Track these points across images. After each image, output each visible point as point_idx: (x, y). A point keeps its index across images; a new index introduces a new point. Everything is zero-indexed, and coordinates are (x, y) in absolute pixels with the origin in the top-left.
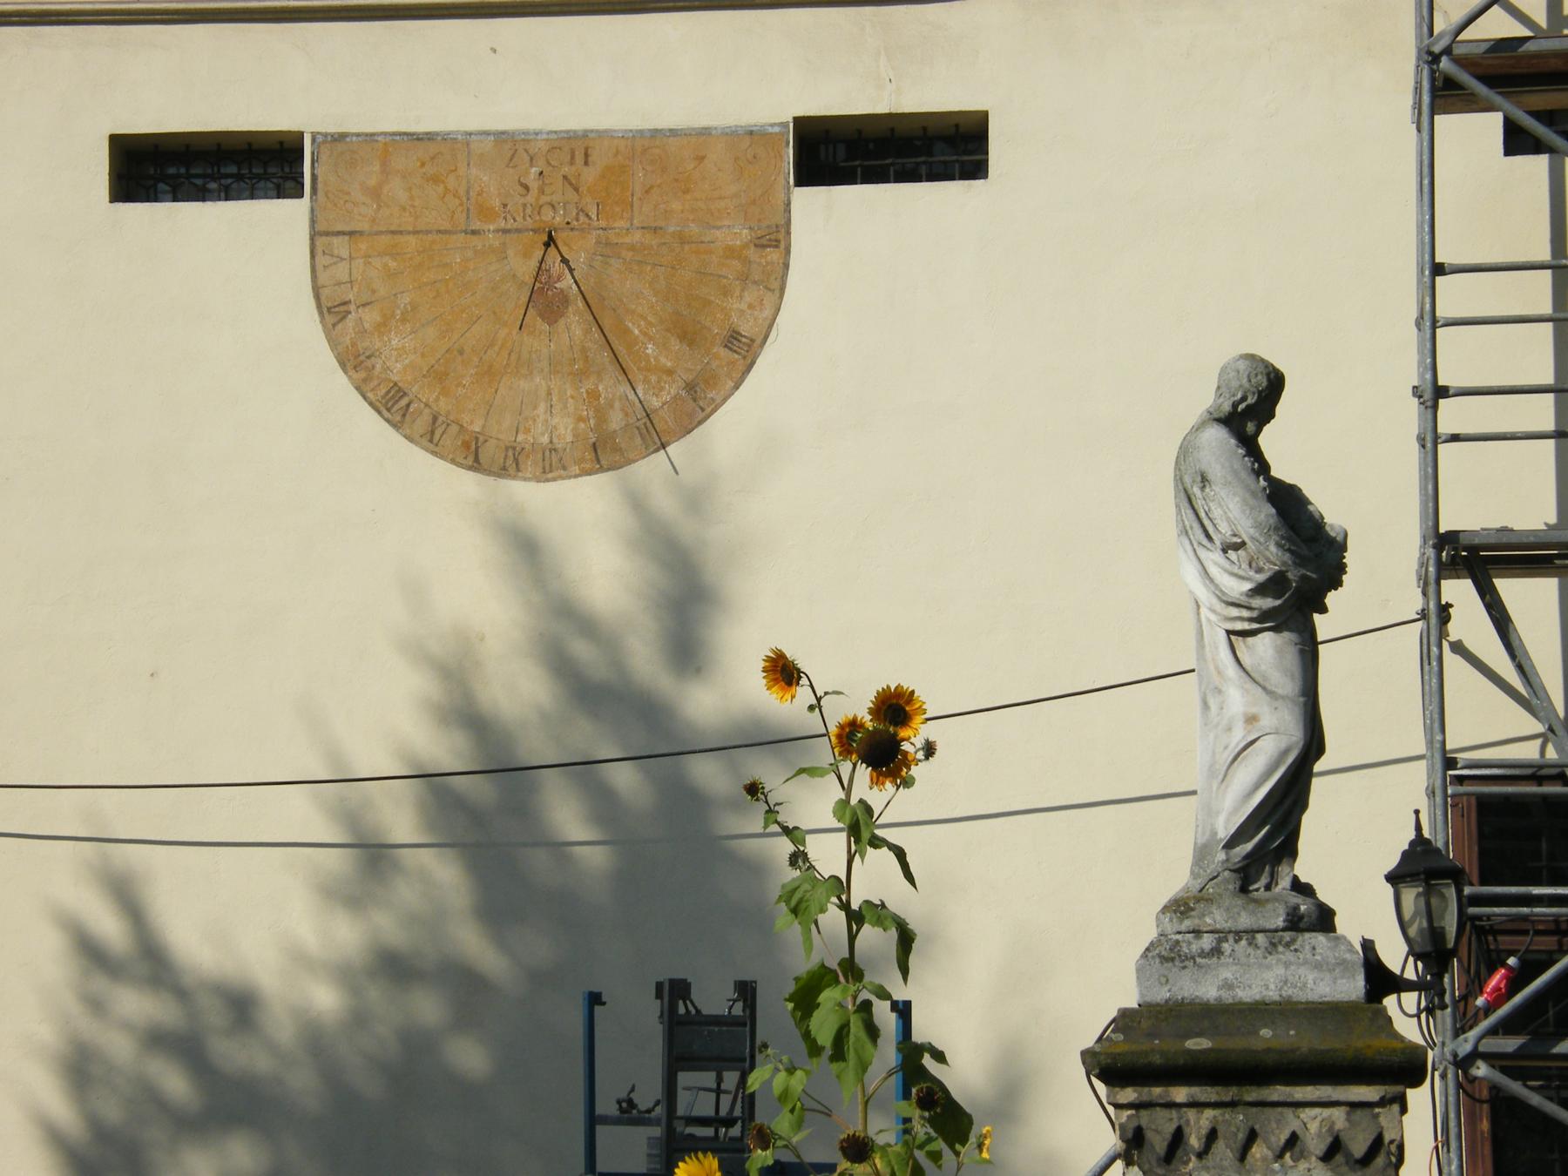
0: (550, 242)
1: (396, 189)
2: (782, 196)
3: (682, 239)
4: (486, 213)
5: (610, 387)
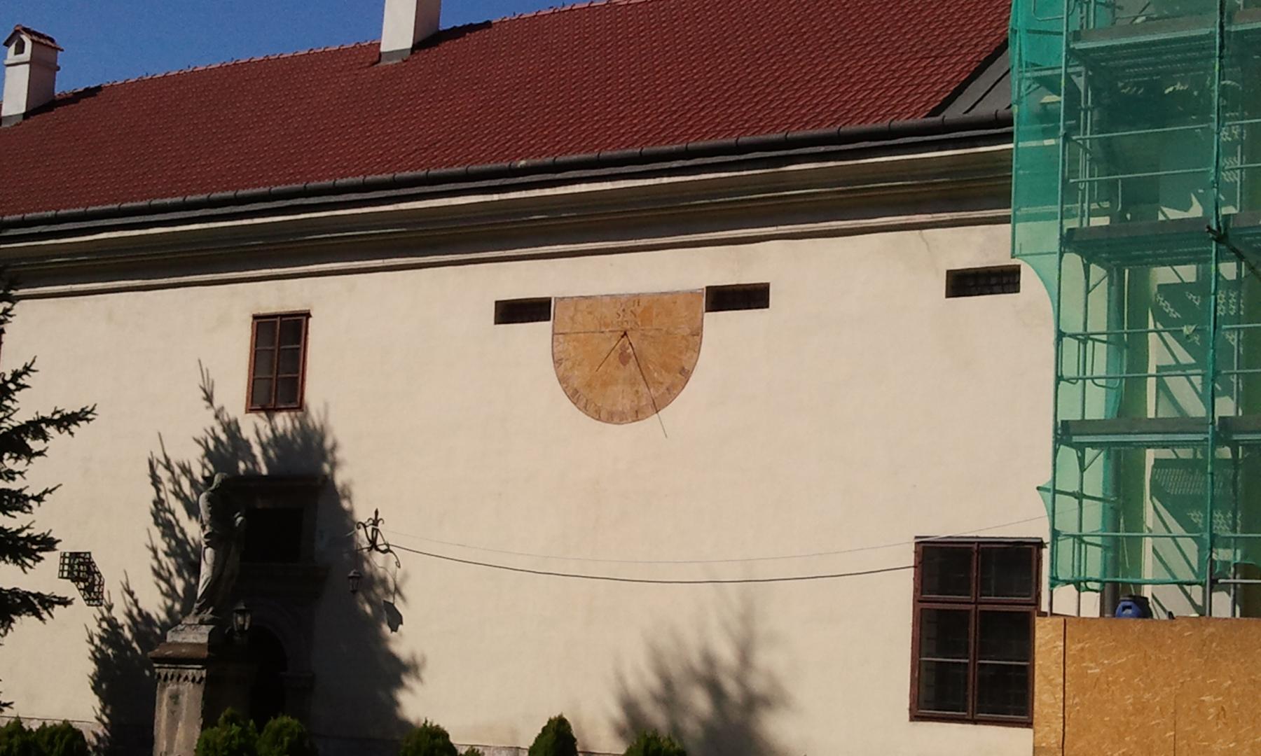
0: (625, 334)
1: (579, 317)
2: (700, 316)
3: (667, 332)
4: (606, 325)
5: (642, 388)
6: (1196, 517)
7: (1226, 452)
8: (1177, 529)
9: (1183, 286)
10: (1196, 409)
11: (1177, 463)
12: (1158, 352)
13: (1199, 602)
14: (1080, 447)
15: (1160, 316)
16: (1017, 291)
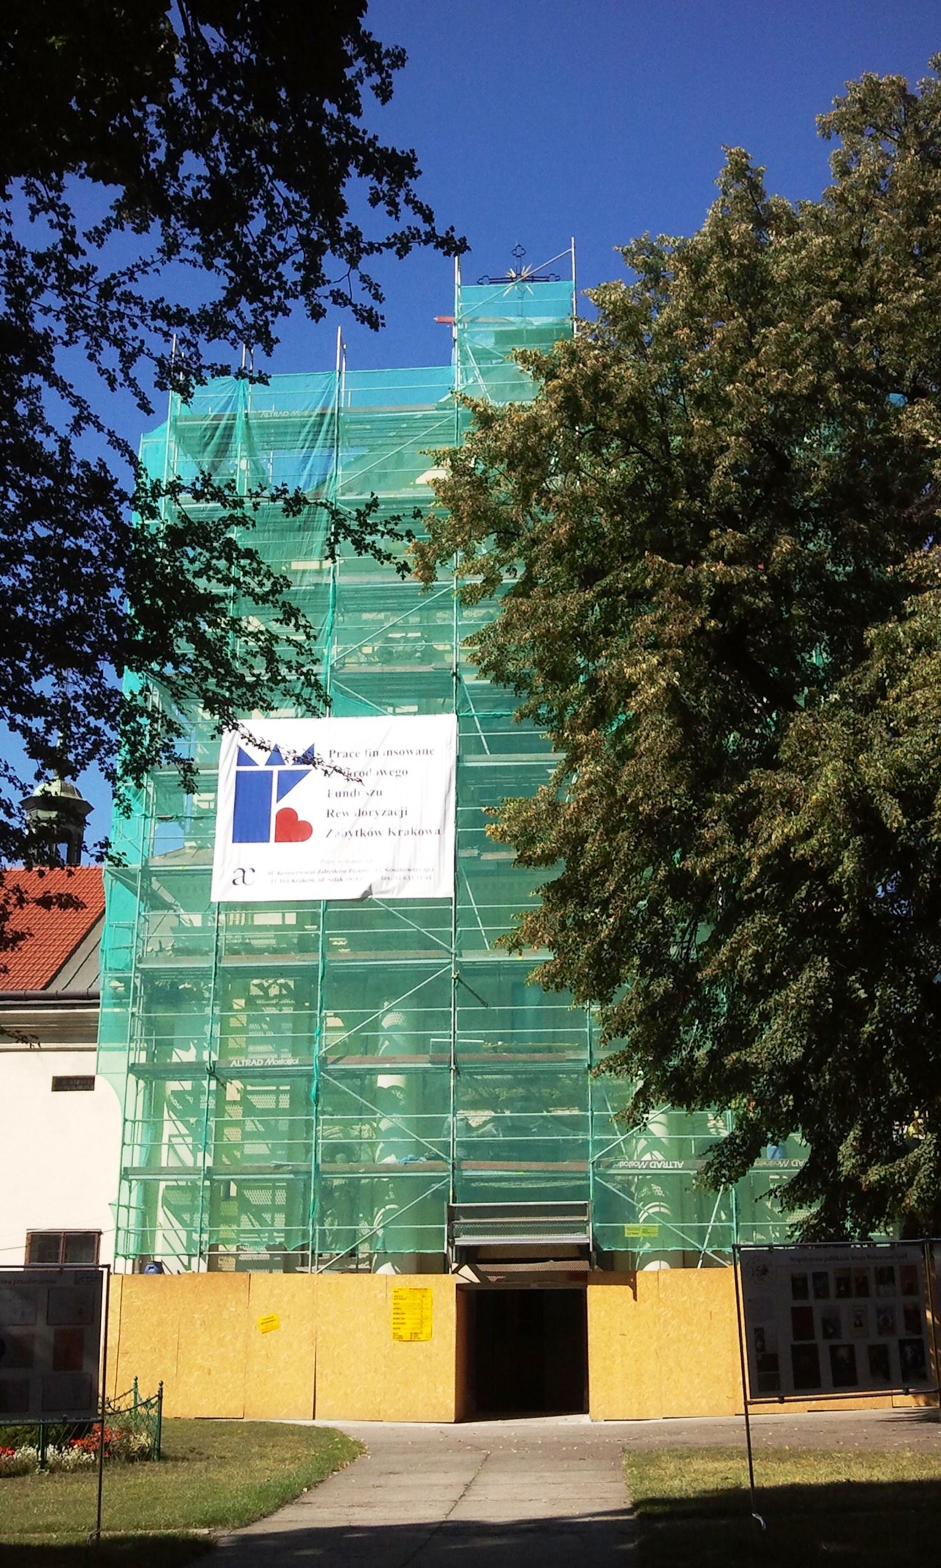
6: (186, 1217)
7: (207, 1183)
8: (177, 1225)
9: (184, 1092)
10: (190, 1162)
11: (179, 1187)
12: (168, 1128)
13: (186, 1263)
14: (130, 1181)
15: (171, 1107)
16: (93, 1090)
